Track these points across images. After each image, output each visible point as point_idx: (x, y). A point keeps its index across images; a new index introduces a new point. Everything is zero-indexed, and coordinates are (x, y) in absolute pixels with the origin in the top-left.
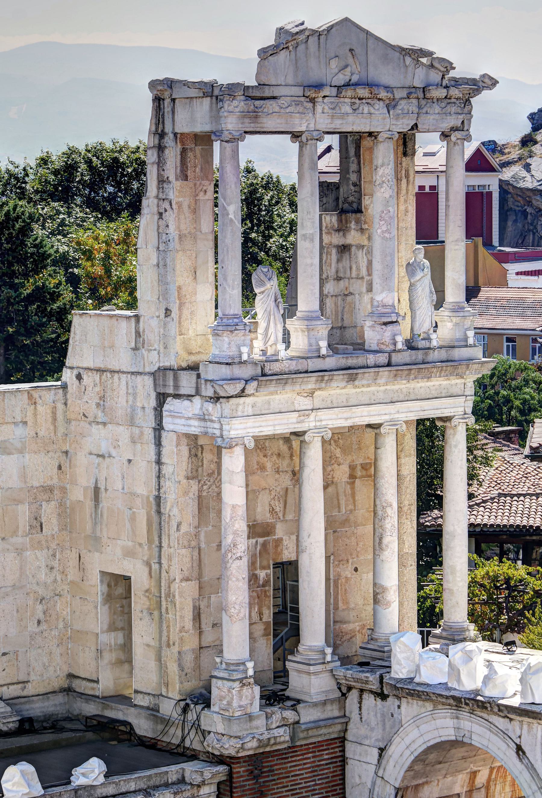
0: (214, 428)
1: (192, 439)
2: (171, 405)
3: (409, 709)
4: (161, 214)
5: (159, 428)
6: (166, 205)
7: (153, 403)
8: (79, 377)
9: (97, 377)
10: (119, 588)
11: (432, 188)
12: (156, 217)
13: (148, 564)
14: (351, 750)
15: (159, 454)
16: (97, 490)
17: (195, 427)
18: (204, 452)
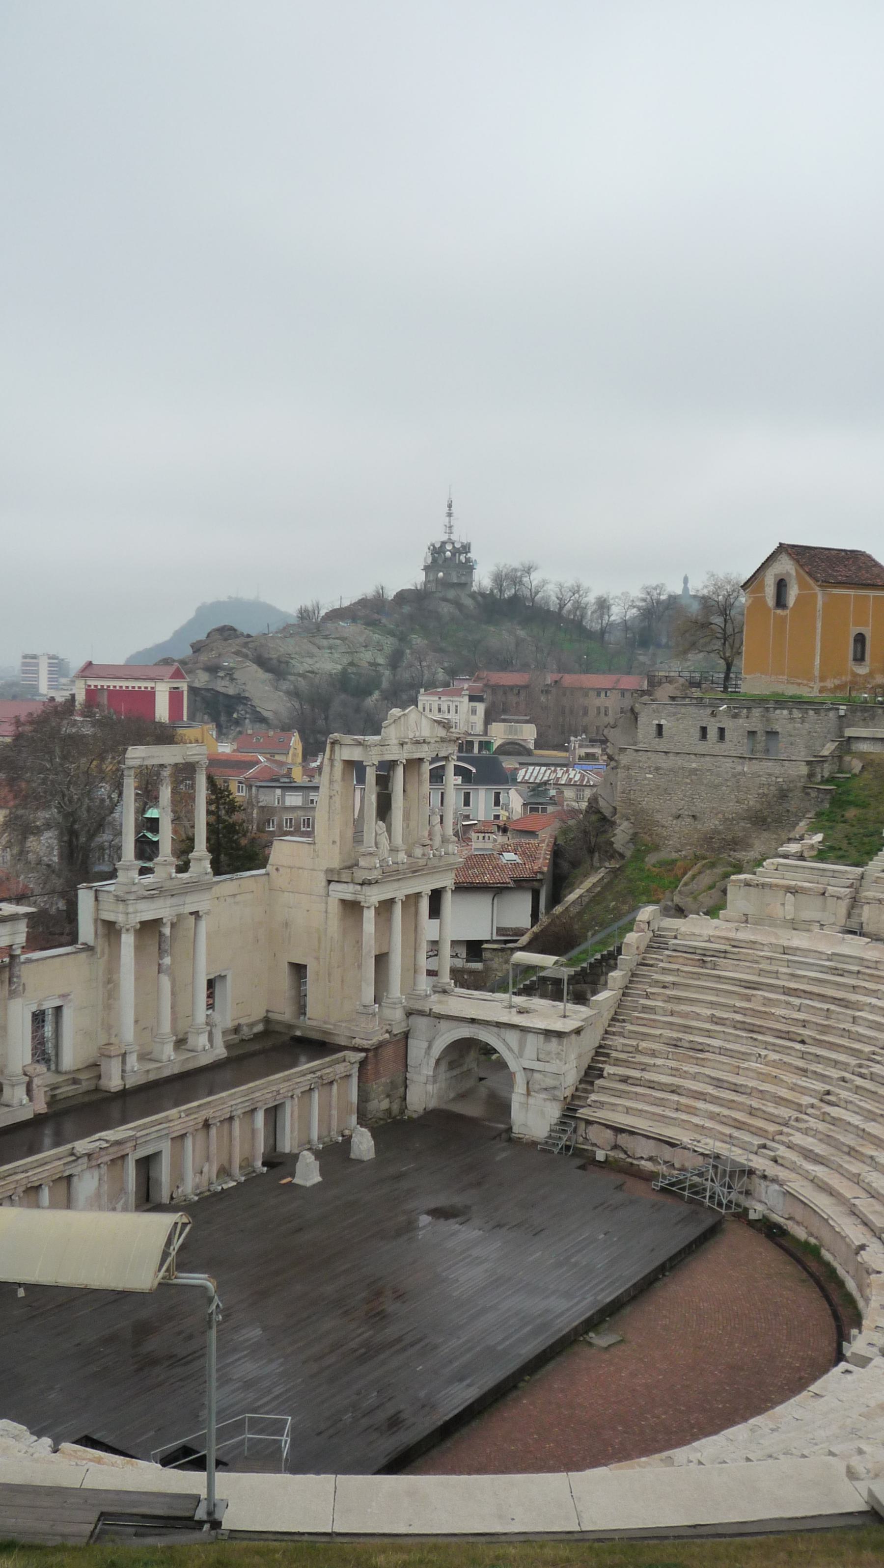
0: (360, 898)
1: (343, 902)
2: (333, 886)
3: (444, 1025)
4: (331, 797)
5: (328, 895)
6: (335, 792)
7: (324, 883)
8: (277, 869)
9: (288, 870)
10: (299, 970)
11: (152, 688)
12: (328, 798)
13: (318, 959)
14: (410, 1041)
15: (327, 908)
16: (287, 923)
17: (349, 897)
18: (352, 908)
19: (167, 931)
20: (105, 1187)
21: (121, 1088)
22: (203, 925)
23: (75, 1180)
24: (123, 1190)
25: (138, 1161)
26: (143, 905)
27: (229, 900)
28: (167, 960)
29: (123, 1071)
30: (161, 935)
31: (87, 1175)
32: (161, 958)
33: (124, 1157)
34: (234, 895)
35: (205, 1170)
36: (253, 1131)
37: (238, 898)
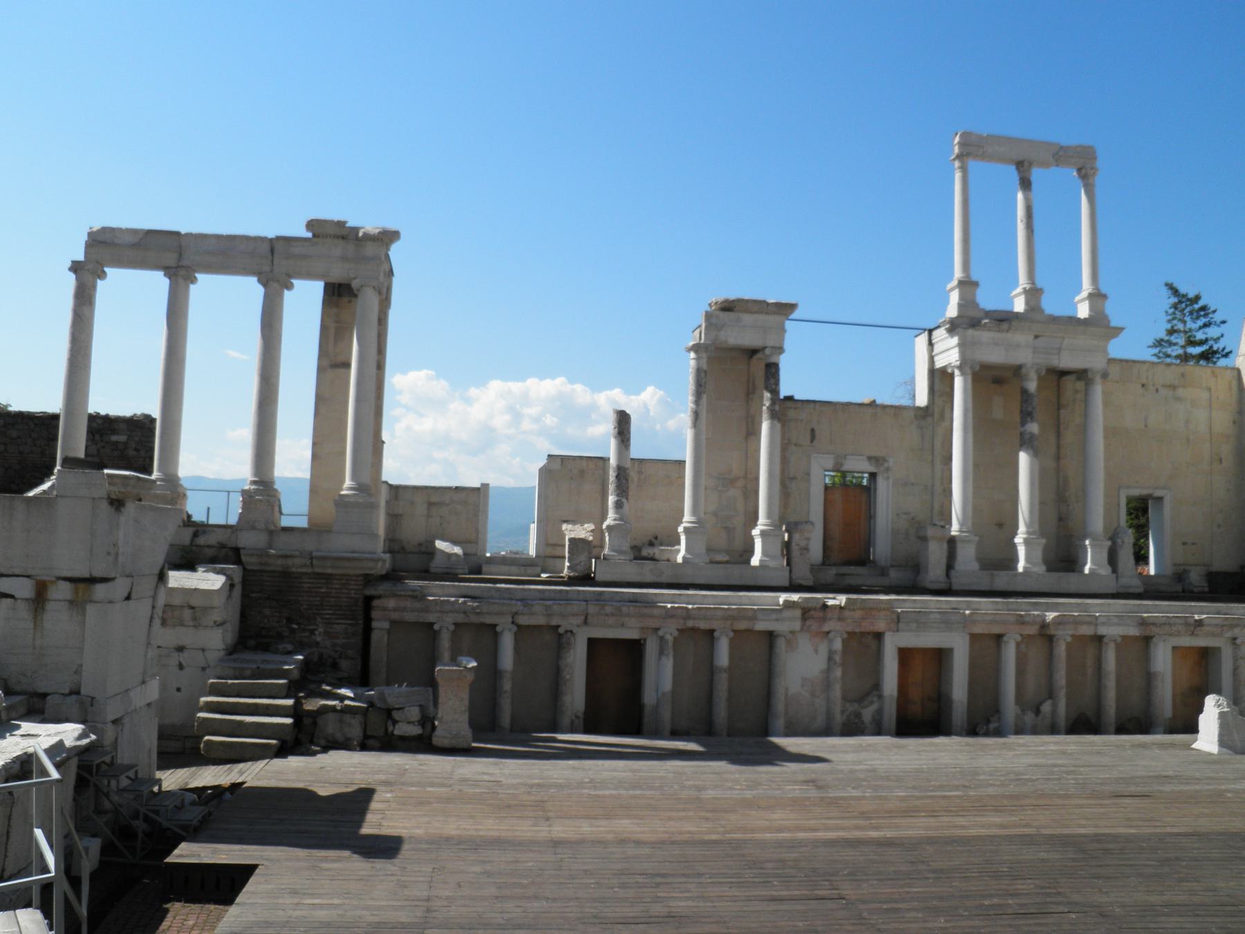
19: (1032, 386)
20: (838, 673)
21: (943, 586)
22: (1098, 391)
23: (781, 644)
24: (877, 686)
25: (905, 655)
26: (985, 336)
27: (1163, 392)
28: (1033, 428)
29: (950, 567)
30: (1024, 392)
31: (805, 644)
32: (1023, 423)
33: (879, 636)
34: (1173, 387)
35: (1046, 707)
36: (1149, 678)
37: (1180, 392)
